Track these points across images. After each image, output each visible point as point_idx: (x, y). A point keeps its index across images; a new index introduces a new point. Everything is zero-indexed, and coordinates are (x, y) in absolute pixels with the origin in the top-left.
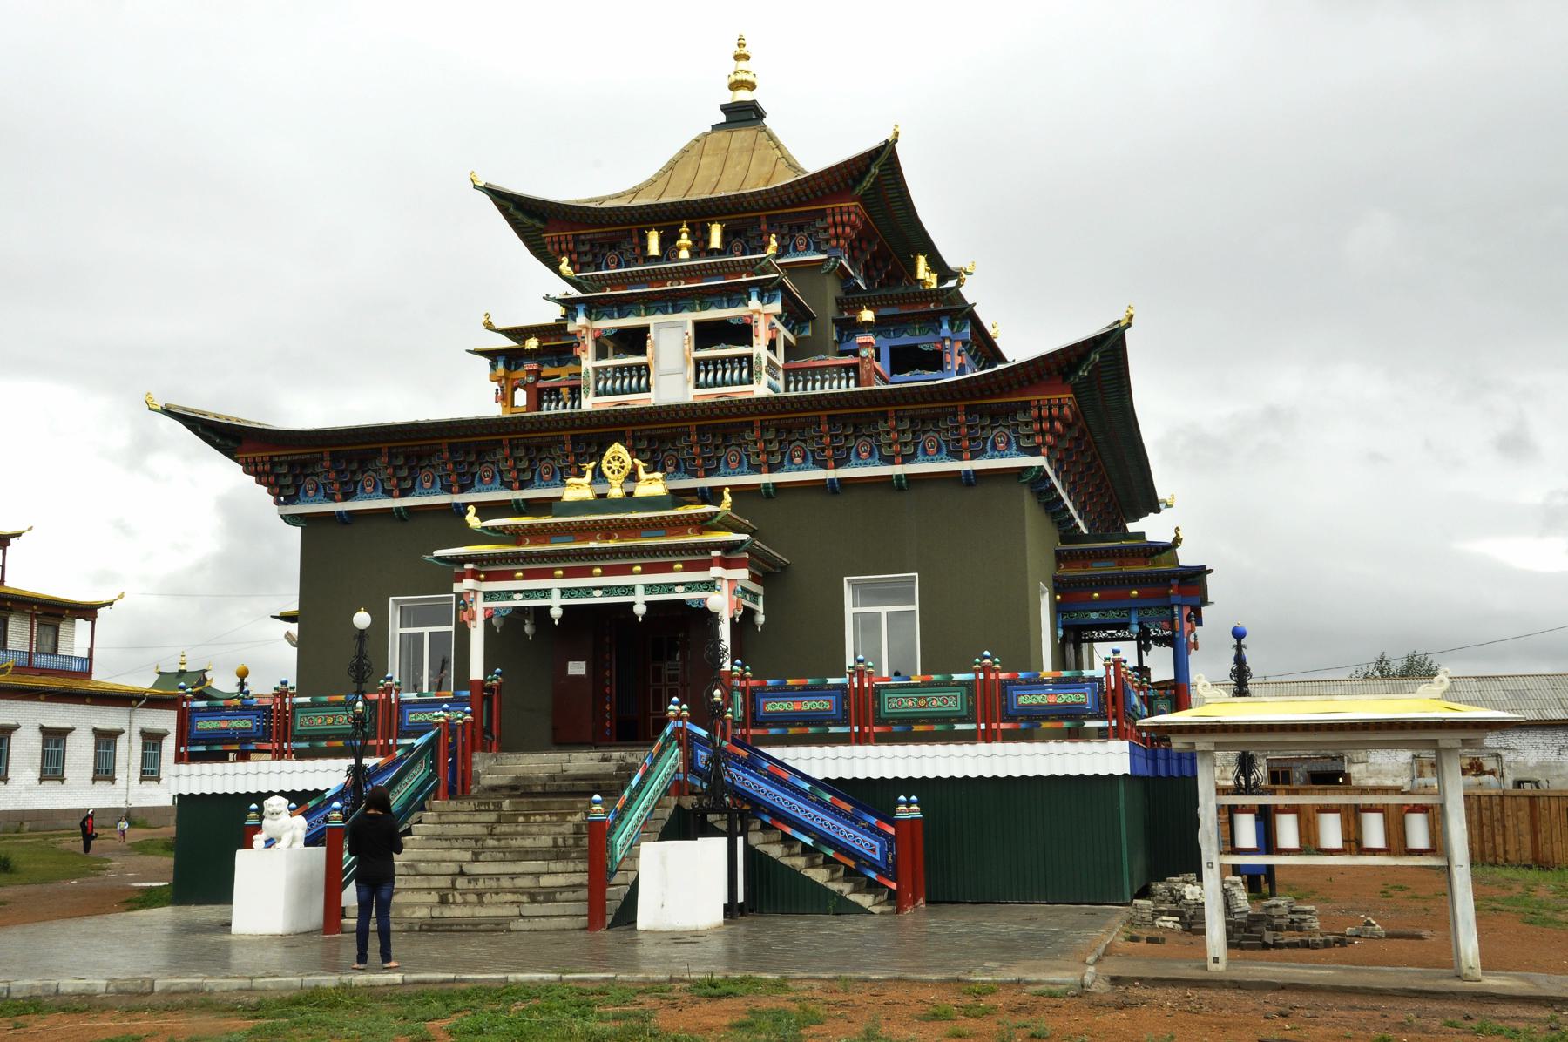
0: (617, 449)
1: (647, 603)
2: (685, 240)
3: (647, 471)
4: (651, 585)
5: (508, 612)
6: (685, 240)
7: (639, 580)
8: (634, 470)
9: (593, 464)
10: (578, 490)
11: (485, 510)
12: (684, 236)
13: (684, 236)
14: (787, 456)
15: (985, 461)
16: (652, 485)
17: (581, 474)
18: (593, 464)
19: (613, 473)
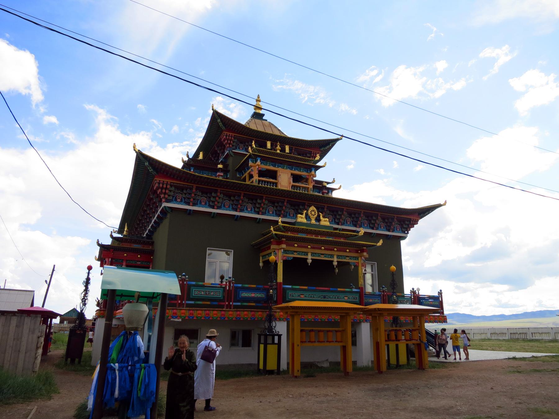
0: (312, 208)
1: (337, 261)
2: (278, 147)
3: (324, 217)
4: (339, 256)
5: (291, 259)
6: (278, 147)
7: (336, 253)
8: (319, 216)
9: (306, 211)
10: (301, 219)
11: (283, 222)
12: (278, 146)
13: (278, 146)
14: (267, 210)
15: (287, 219)
16: (325, 222)
17: (302, 214)
18: (306, 211)
19: (312, 215)
